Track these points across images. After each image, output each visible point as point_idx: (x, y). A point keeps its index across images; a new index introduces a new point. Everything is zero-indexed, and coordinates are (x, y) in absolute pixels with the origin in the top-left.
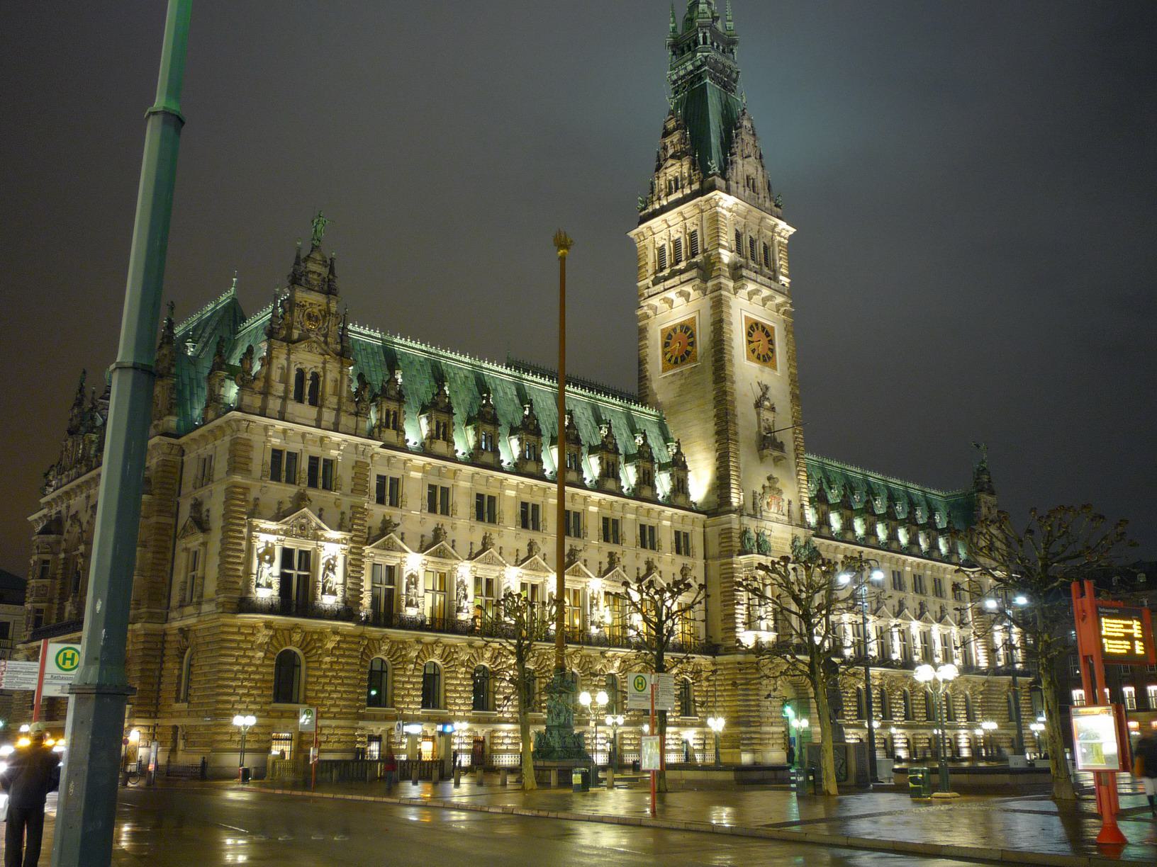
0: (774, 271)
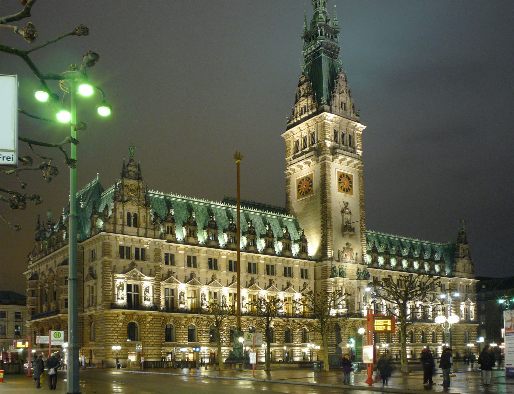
0: (354, 148)
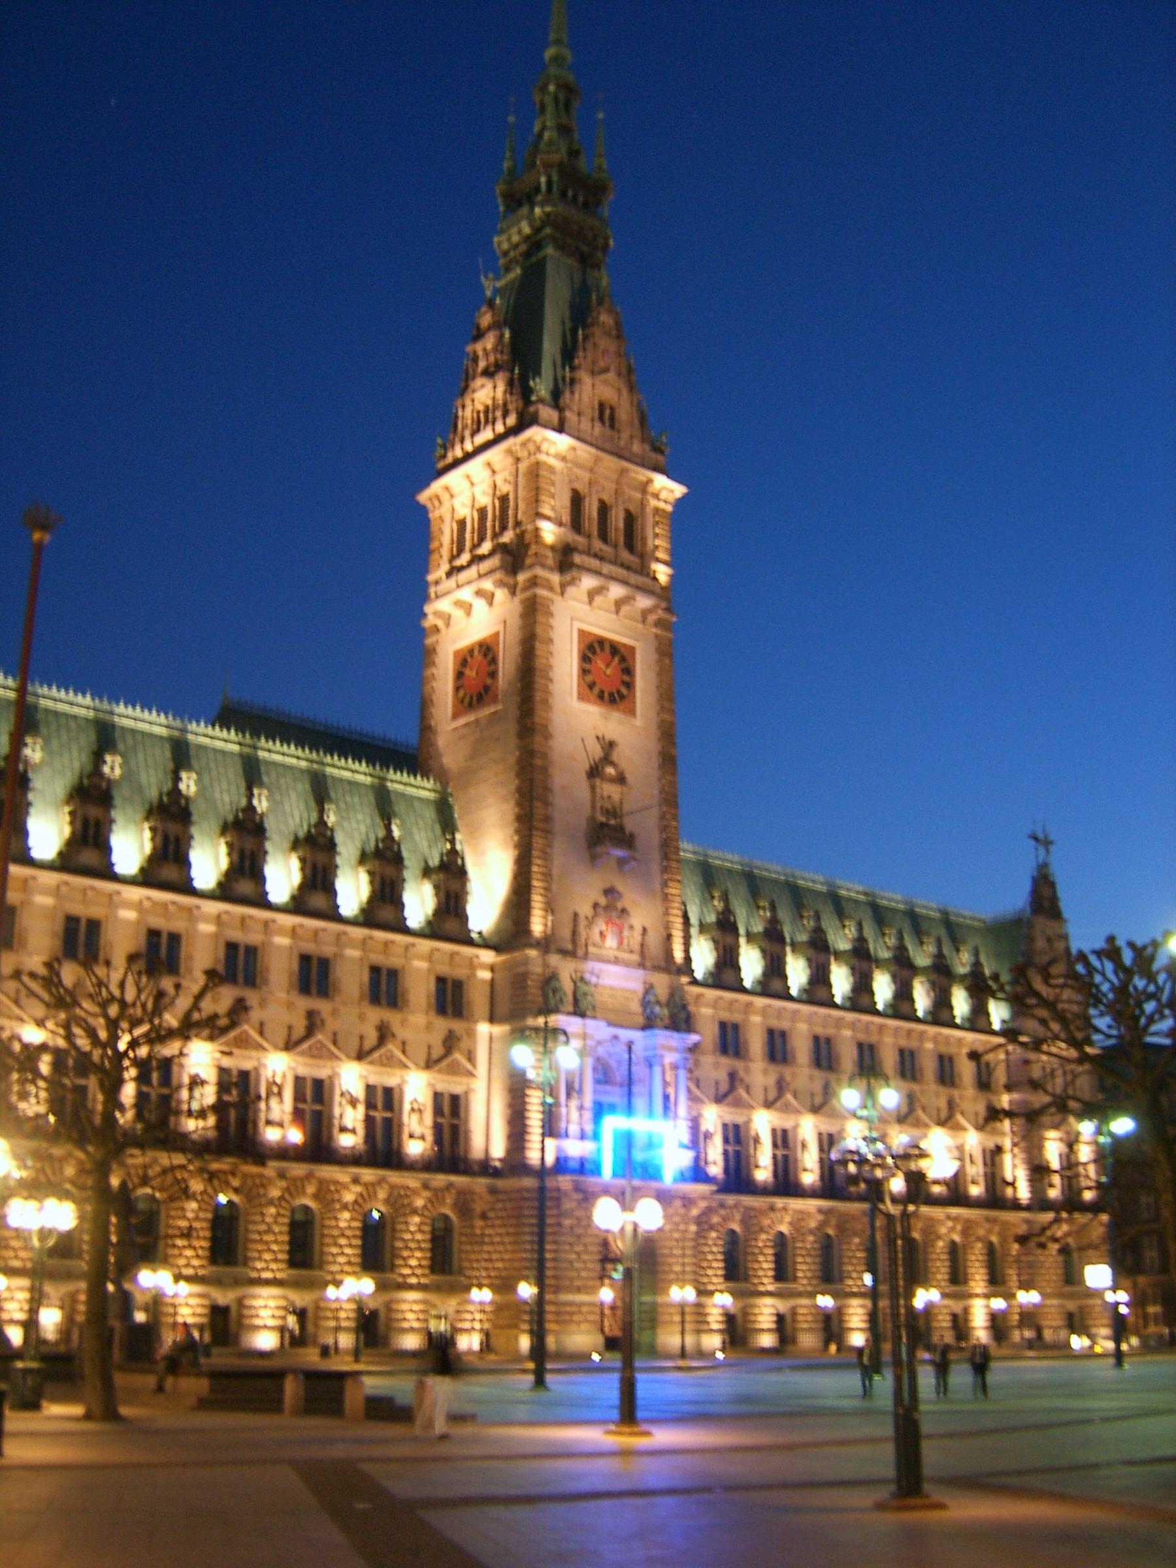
0: (642, 556)
